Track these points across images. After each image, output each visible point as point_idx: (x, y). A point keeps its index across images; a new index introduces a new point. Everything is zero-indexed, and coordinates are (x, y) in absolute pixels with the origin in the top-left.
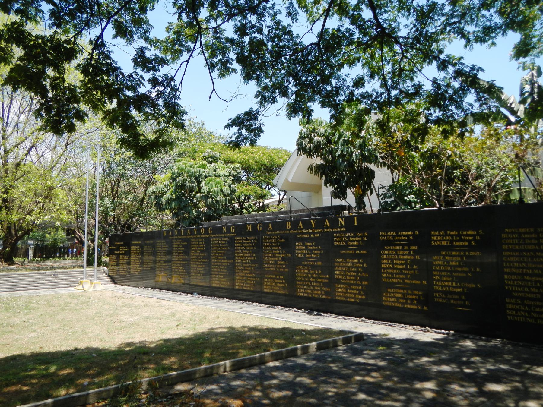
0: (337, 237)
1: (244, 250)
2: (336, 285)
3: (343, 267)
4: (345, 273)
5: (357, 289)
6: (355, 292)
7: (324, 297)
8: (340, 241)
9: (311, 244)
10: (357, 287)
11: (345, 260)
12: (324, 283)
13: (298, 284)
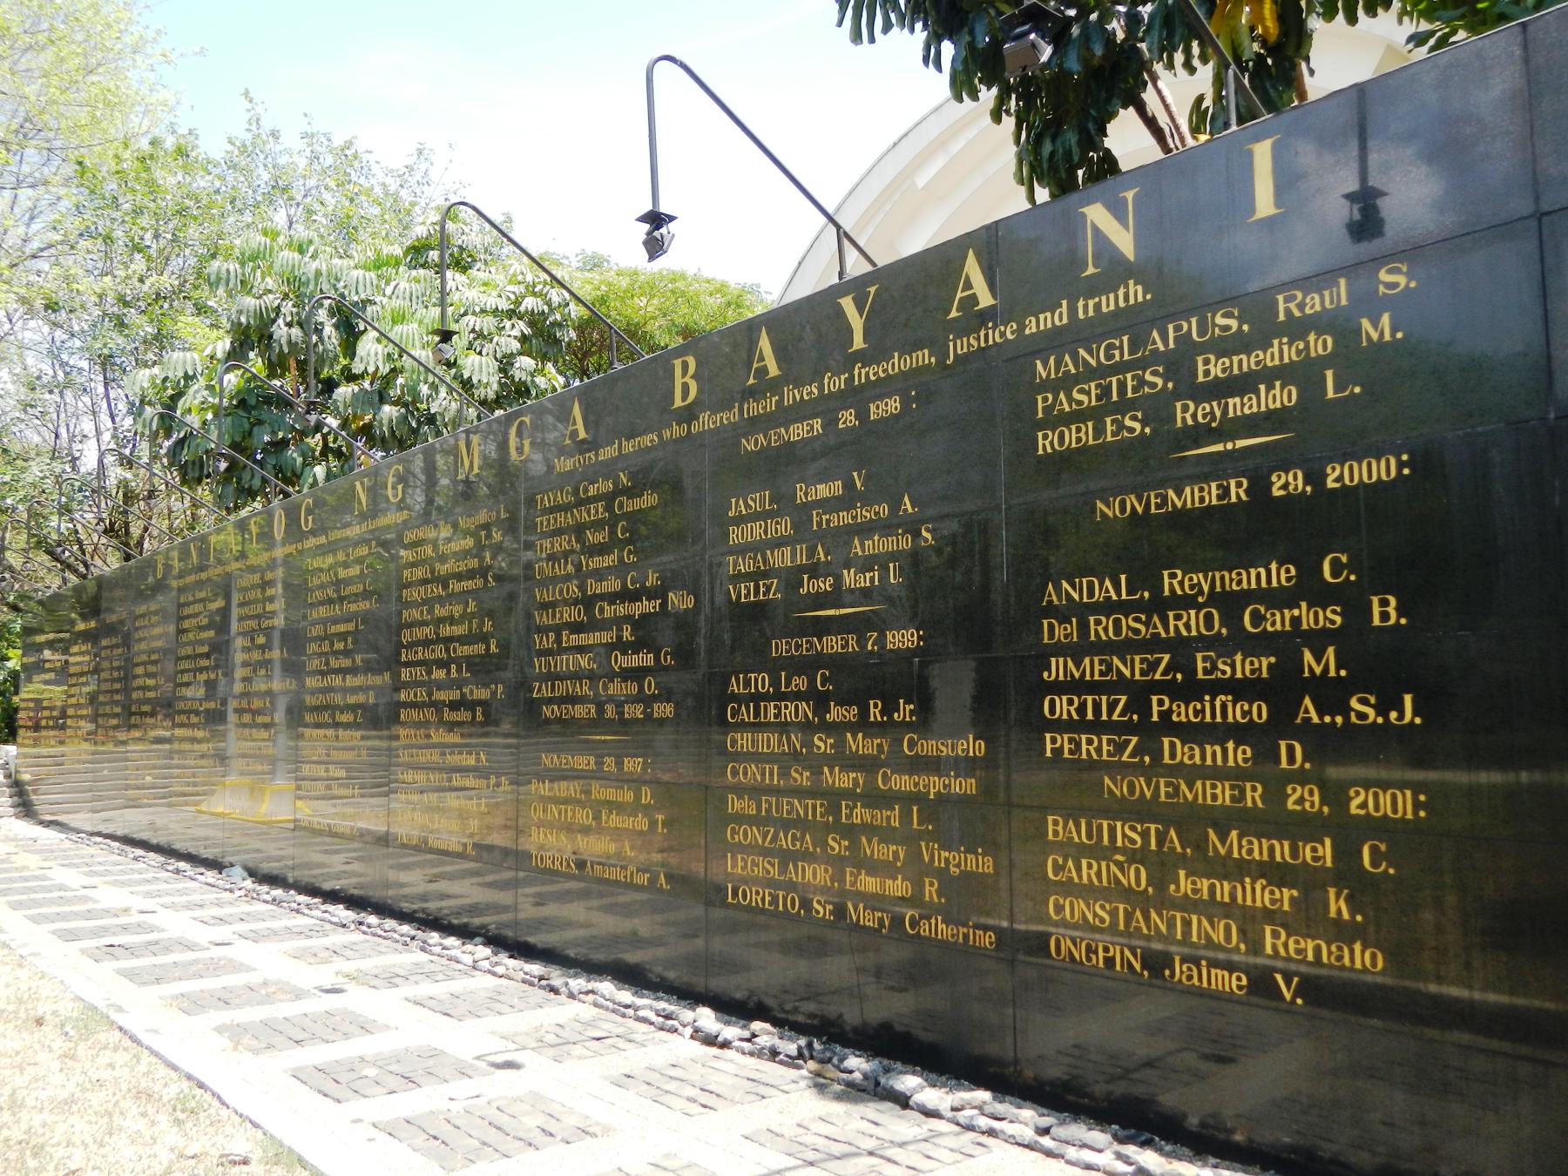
0: (1065, 383)
1: (440, 600)
2: (1054, 827)
3: (1125, 648)
4: (1139, 702)
5: (1276, 874)
6: (1259, 895)
7: (944, 931)
8: (1094, 415)
9: (835, 488)
10: (1282, 851)
11: (1145, 577)
12: (935, 808)
13: (740, 819)
